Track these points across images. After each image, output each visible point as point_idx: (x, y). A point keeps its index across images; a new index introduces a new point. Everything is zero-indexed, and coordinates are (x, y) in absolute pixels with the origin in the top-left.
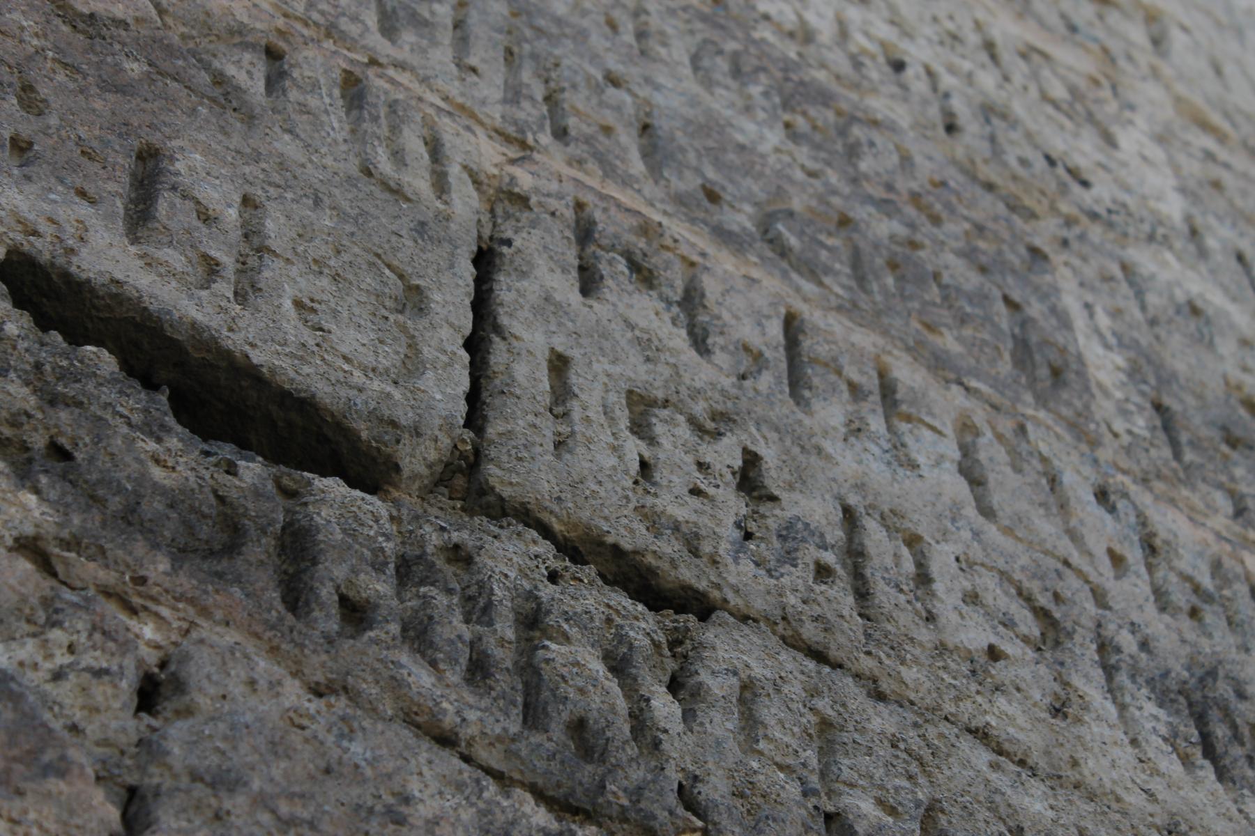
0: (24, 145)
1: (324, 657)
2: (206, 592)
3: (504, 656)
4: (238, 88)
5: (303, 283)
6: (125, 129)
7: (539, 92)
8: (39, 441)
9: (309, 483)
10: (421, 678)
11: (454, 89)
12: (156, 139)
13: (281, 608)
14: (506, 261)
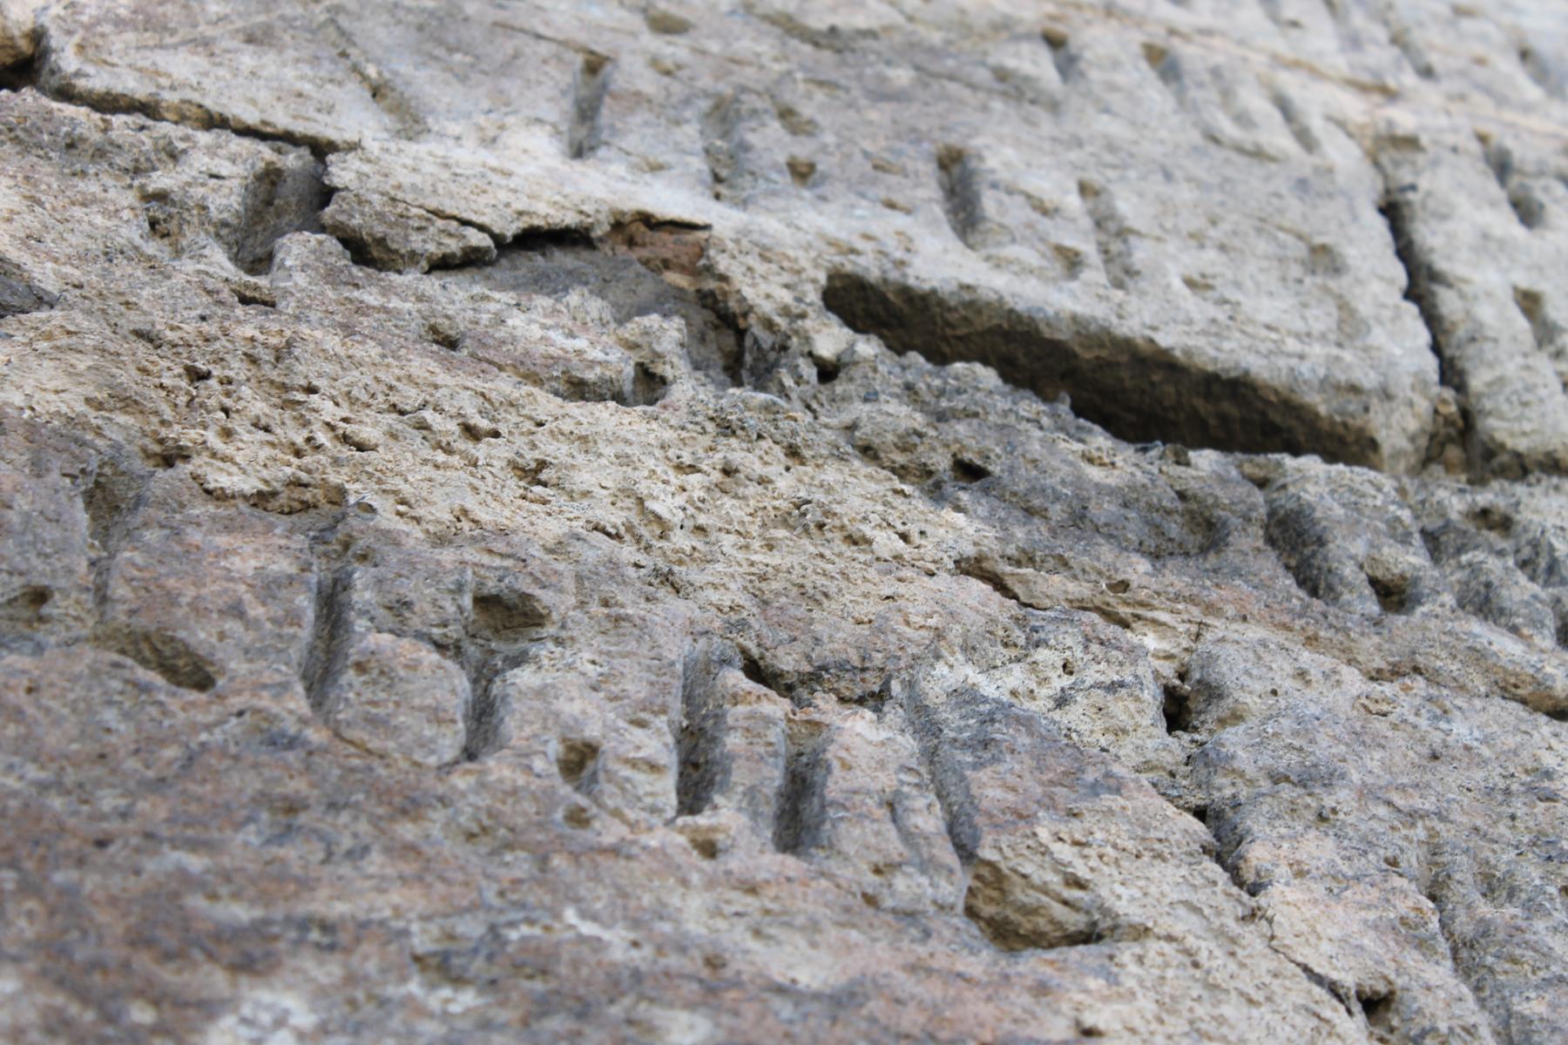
0: (804, 170)
1: (1376, 639)
2: (1204, 587)
4: (1027, 79)
5: (1186, 258)
6: (916, 136)
7: (1381, 34)
8: (941, 462)
9: (1279, 464)
10: (1505, 646)
11: (1281, 46)
12: (954, 140)
13: (1302, 594)
14: (1417, 206)
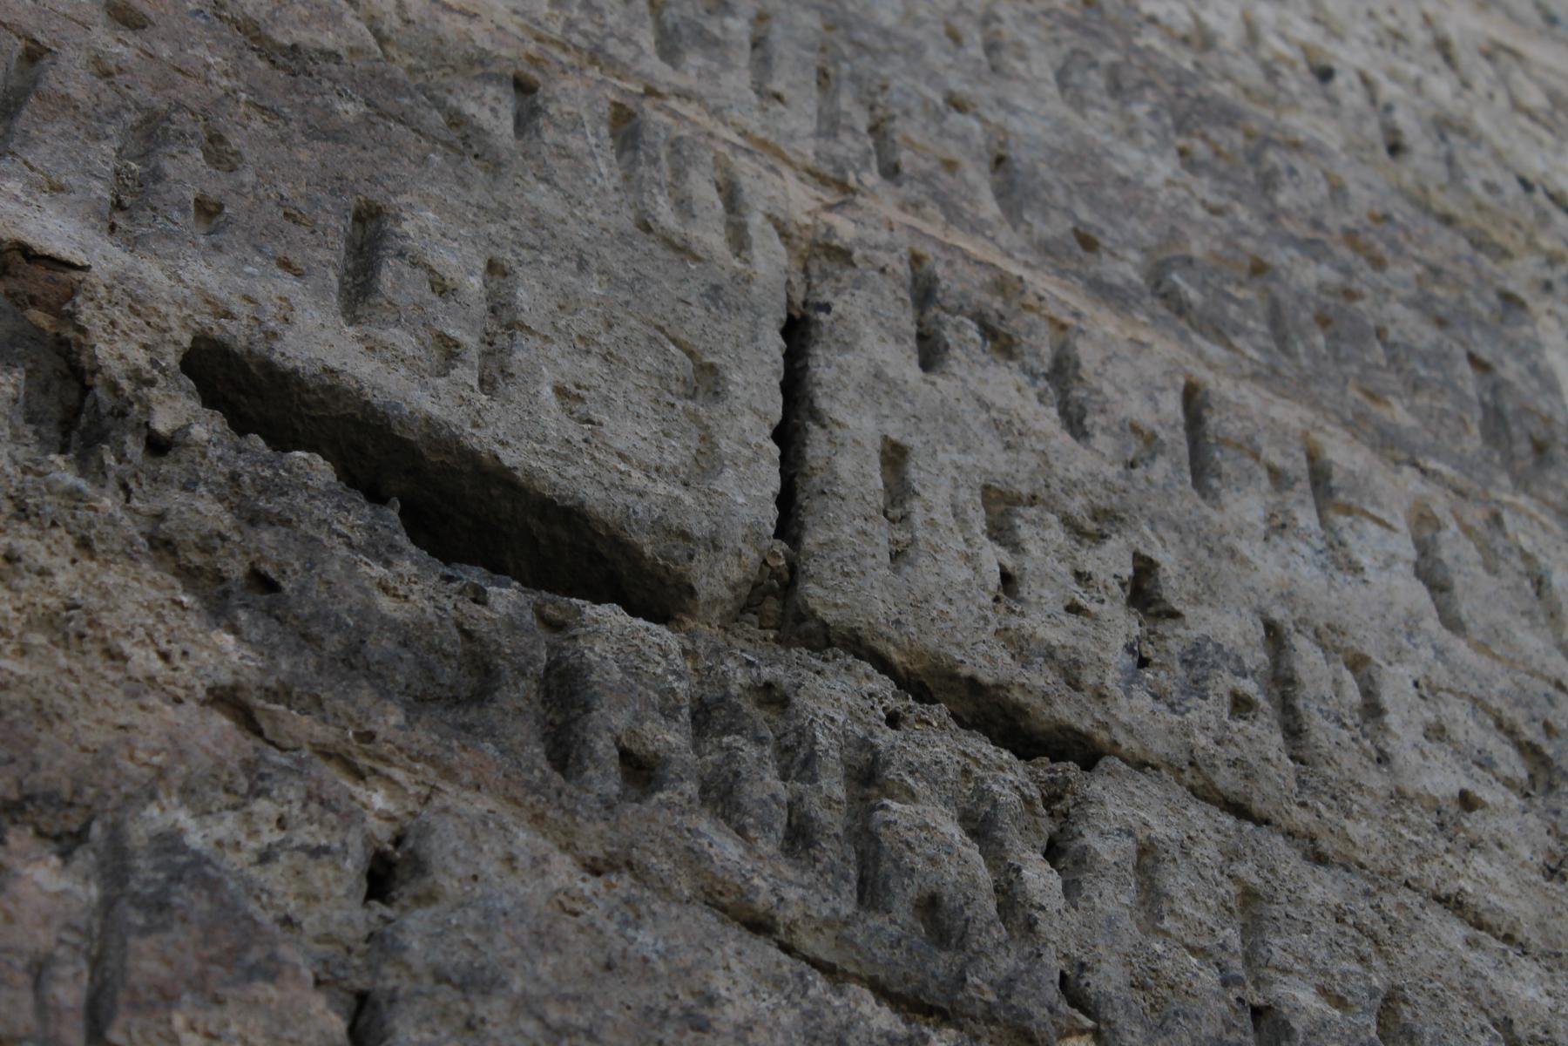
0: (212, 208)
1: (601, 826)
2: (450, 749)
3: (832, 820)
4: (480, 130)
5: (565, 365)
6: (339, 184)
7: (862, 121)
8: (236, 569)
9: (579, 612)
10: (726, 849)
11: (754, 122)
12: (377, 195)
13: (546, 766)
14: (824, 330)
